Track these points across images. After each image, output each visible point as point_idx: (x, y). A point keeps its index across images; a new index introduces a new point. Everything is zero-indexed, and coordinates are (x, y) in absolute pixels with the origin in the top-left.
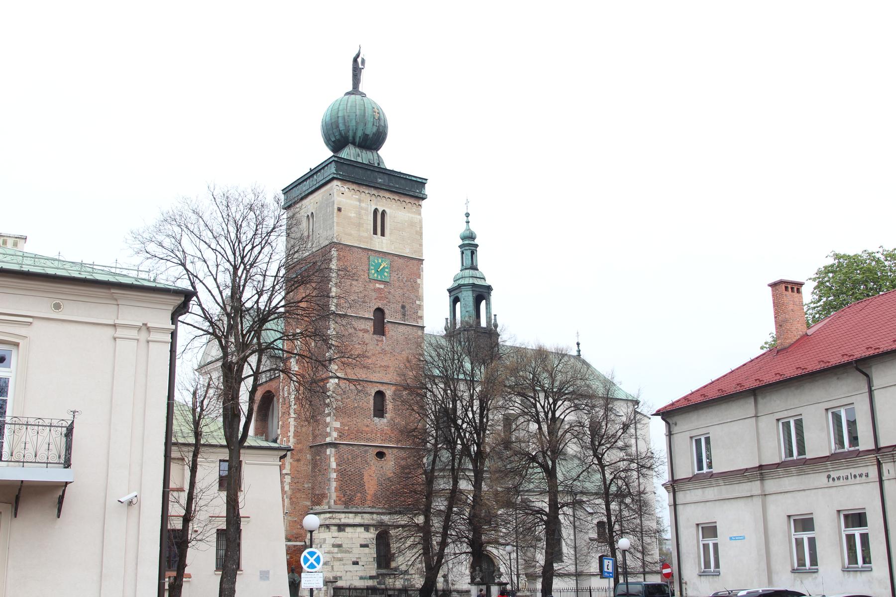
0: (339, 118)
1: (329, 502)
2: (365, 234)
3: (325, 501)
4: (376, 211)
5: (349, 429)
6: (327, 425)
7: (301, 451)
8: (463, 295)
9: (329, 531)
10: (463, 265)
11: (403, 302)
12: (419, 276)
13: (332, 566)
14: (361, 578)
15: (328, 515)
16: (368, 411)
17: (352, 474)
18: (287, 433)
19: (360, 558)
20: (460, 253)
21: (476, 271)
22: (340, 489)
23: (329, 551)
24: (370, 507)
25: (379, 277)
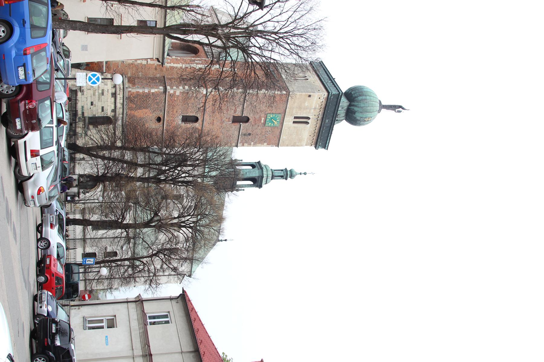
0: (366, 97)
1: (130, 87)
2: (294, 112)
3: (131, 85)
4: (308, 118)
5: (175, 100)
6: (178, 87)
7: (162, 70)
8: (256, 170)
9: (112, 88)
10: (275, 170)
11: (253, 134)
12: (268, 144)
13: (90, 89)
14: (83, 107)
15: (122, 87)
16: (186, 112)
17: (147, 102)
18: (173, 62)
19: (95, 106)
20: (282, 169)
21: (271, 178)
22: (138, 94)
23: (100, 87)
24: (127, 113)
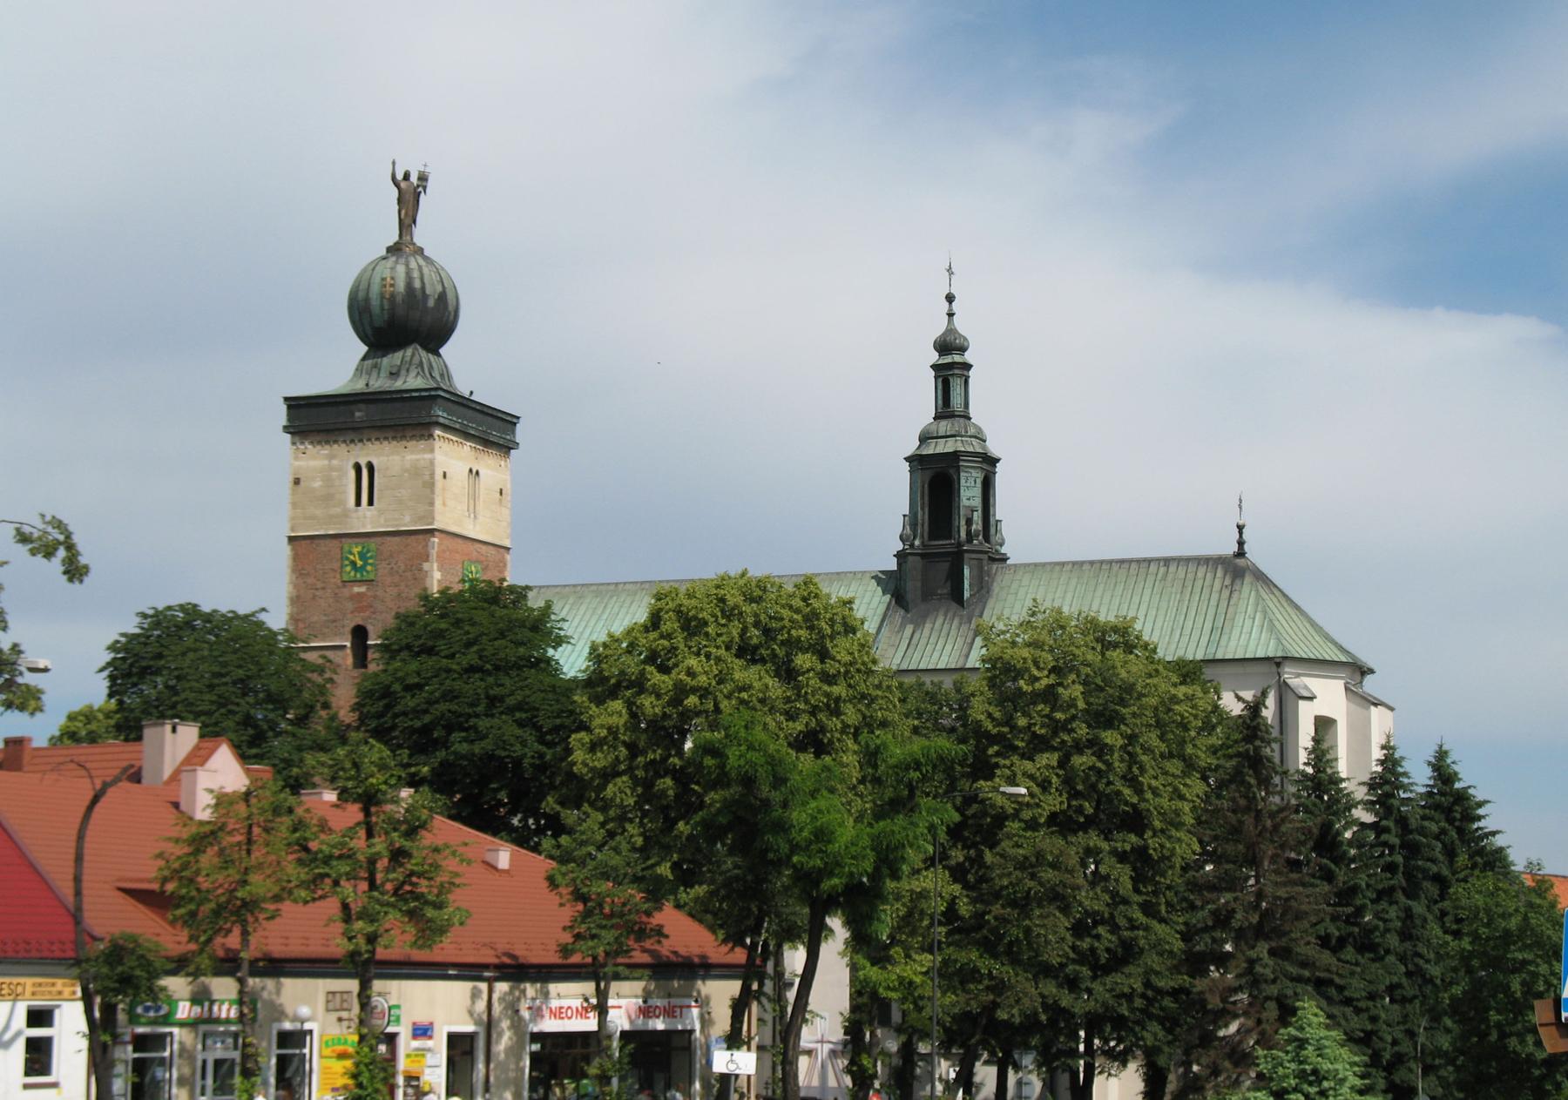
25: (358, 575)
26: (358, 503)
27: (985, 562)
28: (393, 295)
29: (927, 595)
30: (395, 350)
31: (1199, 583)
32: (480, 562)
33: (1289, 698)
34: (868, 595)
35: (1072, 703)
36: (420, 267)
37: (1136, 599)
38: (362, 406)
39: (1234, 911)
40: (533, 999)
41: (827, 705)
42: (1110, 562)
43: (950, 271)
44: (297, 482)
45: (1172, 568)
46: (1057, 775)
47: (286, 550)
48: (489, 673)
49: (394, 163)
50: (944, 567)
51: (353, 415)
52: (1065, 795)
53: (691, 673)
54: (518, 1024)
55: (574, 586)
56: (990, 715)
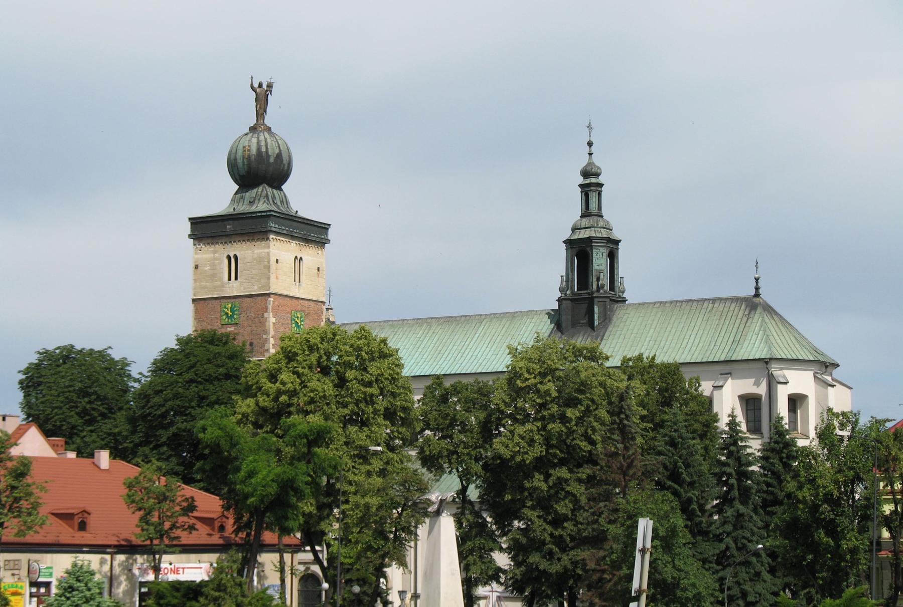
25: (232, 321)
26: (230, 279)
27: (608, 303)
28: (249, 157)
29: (575, 323)
30: (253, 189)
31: (730, 314)
32: (304, 311)
33: (772, 383)
34: (542, 324)
35: (548, 393)
36: (266, 139)
37: (693, 324)
38: (231, 222)
39: (602, 513)
40: (142, 564)
41: (365, 399)
42: (682, 302)
43: (590, 127)
44: (197, 267)
45: (716, 305)
46: (542, 435)
47: (191, 307)
48: (201, 383)
49: (252, 77)
50: (584, 307)
51: (226, 227)
52: (544, 447)
53: (283, 383)
54: (131, 577)
55: (380, 322)
56: (504, 401)
